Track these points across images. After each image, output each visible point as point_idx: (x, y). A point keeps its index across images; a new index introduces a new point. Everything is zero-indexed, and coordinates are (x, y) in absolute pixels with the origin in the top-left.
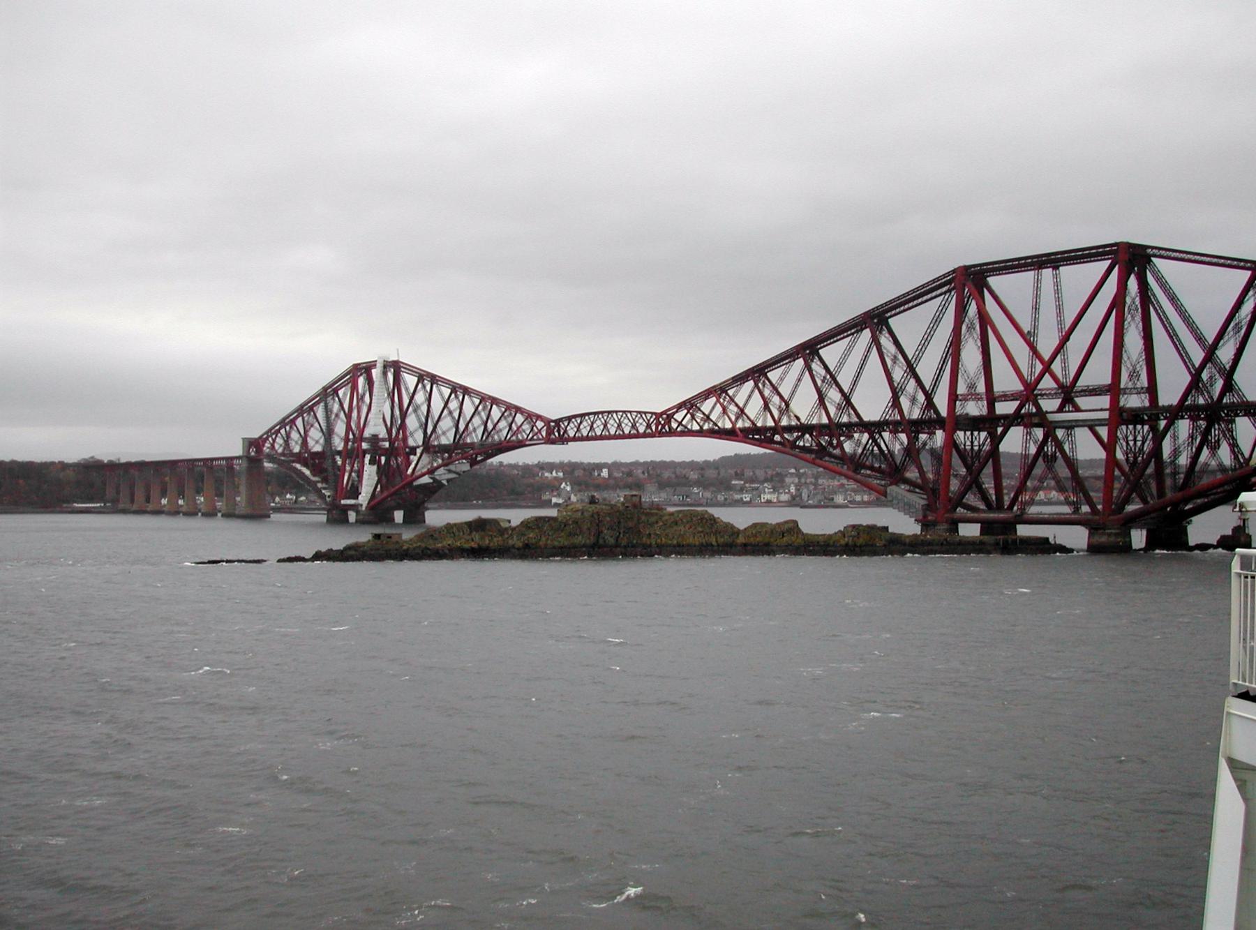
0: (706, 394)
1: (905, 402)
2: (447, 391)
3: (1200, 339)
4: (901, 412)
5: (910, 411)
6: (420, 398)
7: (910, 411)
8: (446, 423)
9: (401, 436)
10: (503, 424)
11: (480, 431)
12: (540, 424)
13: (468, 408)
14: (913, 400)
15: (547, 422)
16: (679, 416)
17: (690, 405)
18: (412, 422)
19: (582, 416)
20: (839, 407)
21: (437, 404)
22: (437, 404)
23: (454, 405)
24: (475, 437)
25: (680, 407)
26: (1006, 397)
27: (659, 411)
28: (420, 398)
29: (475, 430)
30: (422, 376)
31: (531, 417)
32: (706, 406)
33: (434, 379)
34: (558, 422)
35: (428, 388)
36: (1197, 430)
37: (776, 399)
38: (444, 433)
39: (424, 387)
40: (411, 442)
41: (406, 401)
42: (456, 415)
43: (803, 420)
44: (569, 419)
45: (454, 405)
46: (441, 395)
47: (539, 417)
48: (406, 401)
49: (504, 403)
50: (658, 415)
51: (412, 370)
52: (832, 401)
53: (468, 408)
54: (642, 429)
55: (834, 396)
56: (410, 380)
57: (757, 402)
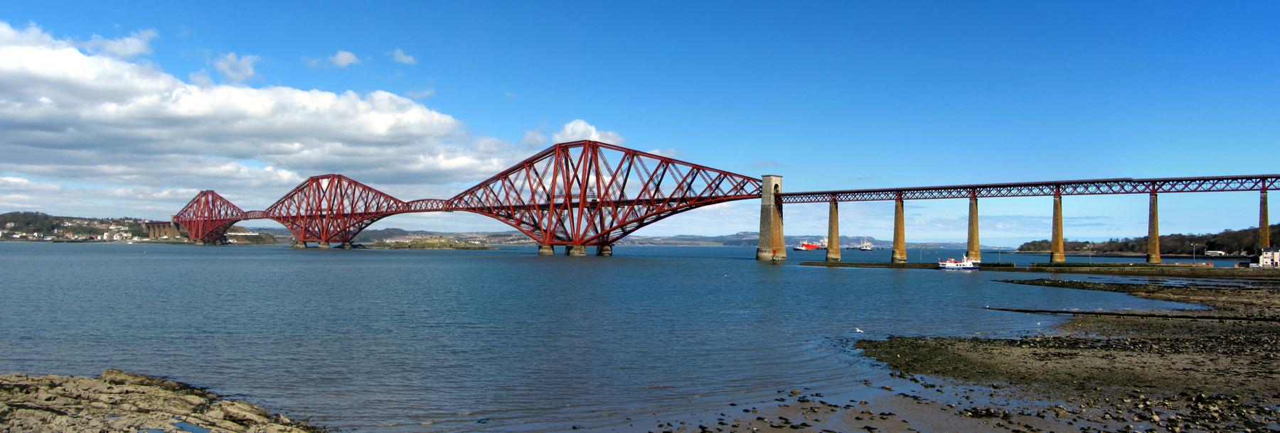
0: (466, 193)
1: (537, 198)
2: (361, 189)
3: (648, 173)
4: (535, 202)
5: (539, 201)
6: (349, 191)
7: (539, 201)
8: (361, 203)
9: (341, 208)
10: (385, 204)
11: (376, 207)
12: (400, 205)
13: (371, 196)
14: (541, 197)
15: (403, 203)
16: (456, 202)
17: (460, 197)
18: (346, 202)
19: (418, 201)
20: (477, 202)
21: (357, 194)
22: (357, 194)
23: (364, 195)
24: (373, 210)
25: (455, 198)
26: (576, 196)
27: (447, 199)
28: (349, 191)
29: (373, 207)
30: (351, 182)
31: (396, 201)
32: (466, 198)
33: (356, 184)
34: (408, 204)
35: (353, 187)
36: (653, 210)
37: (492, 195)
38: (360, 208)
39: (351, 187)
40: (346, 212)
41: (343, 192)
42: (365, 200)
43: (526, 204)
44: (413, 202)
45: (364, 195)
46: (359, 189)
47: (400, 202)
48: (343, 192)
49: (385, 195)
50: (447, 202)
51: (346, 179)
52: (511, 197)
53: (371, 196)
54: (441, 207)
55: (513, 194)
56: (345, 184)
57: (485, 196)
